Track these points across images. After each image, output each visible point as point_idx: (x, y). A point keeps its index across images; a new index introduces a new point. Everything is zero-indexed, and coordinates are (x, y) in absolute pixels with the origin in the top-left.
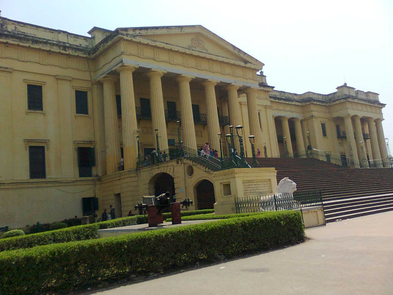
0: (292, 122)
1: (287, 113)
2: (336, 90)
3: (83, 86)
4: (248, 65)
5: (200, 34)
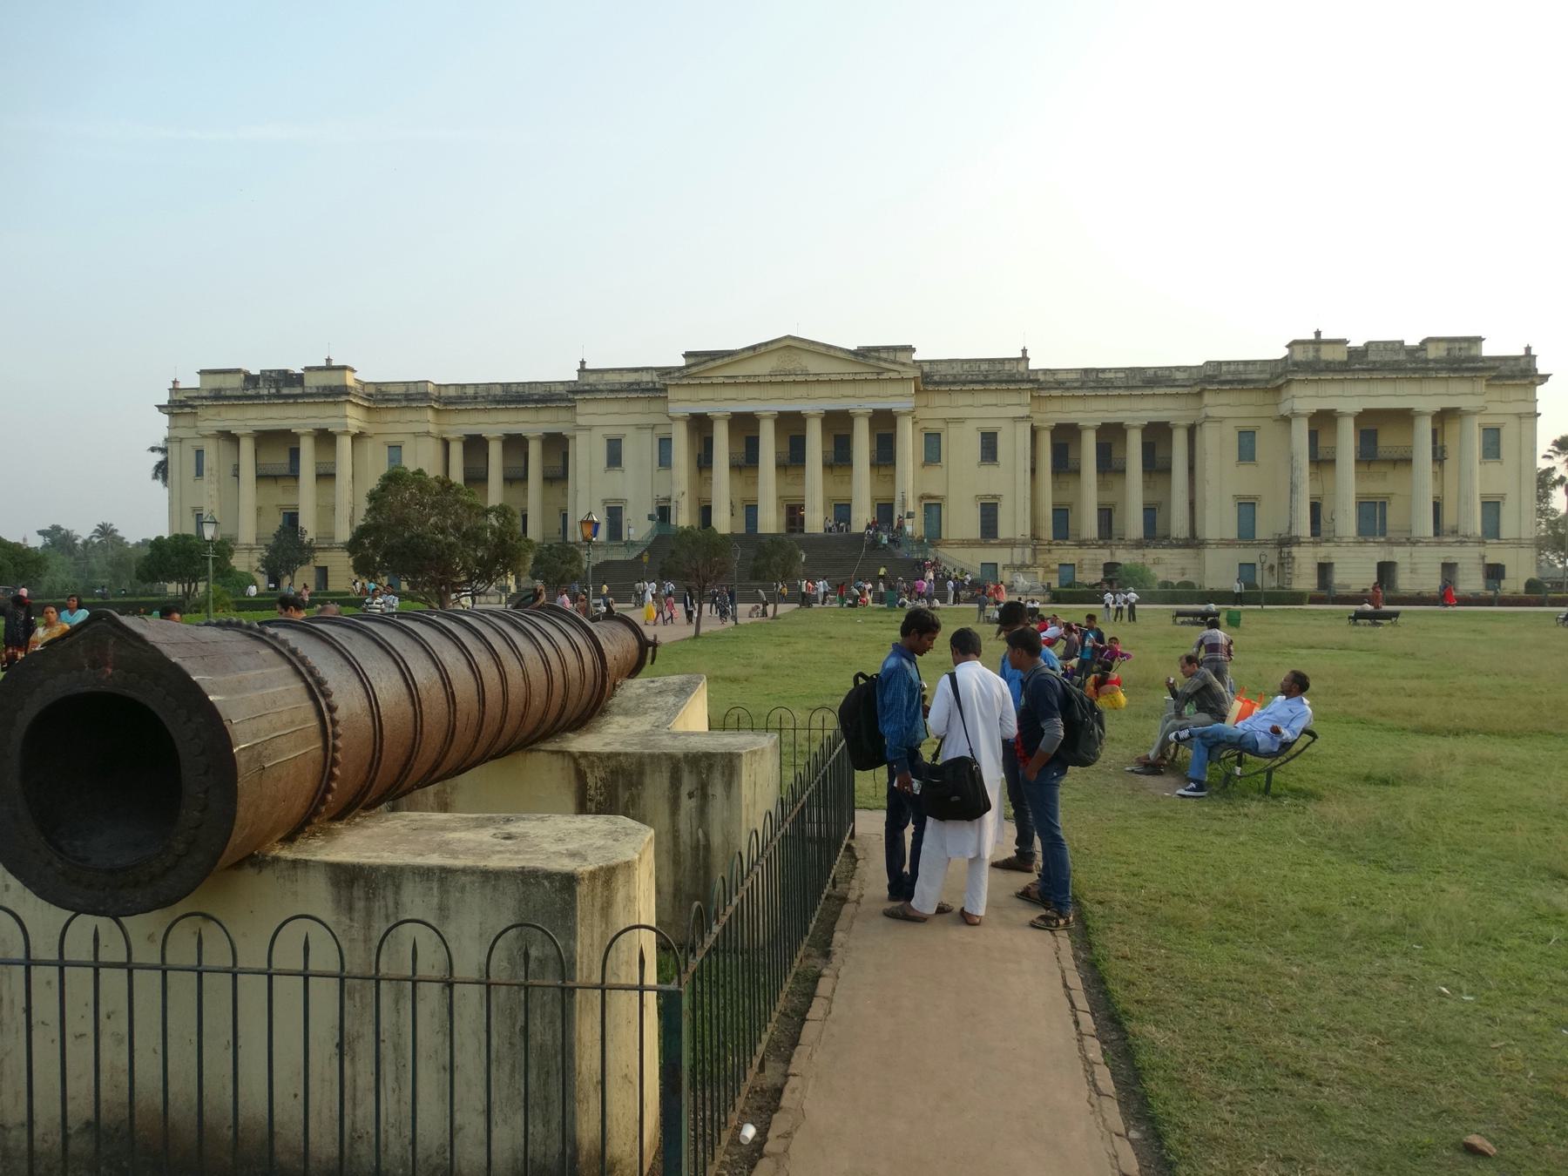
0: (1157, 434)
2: (1286, 352)
4: (885, 376)
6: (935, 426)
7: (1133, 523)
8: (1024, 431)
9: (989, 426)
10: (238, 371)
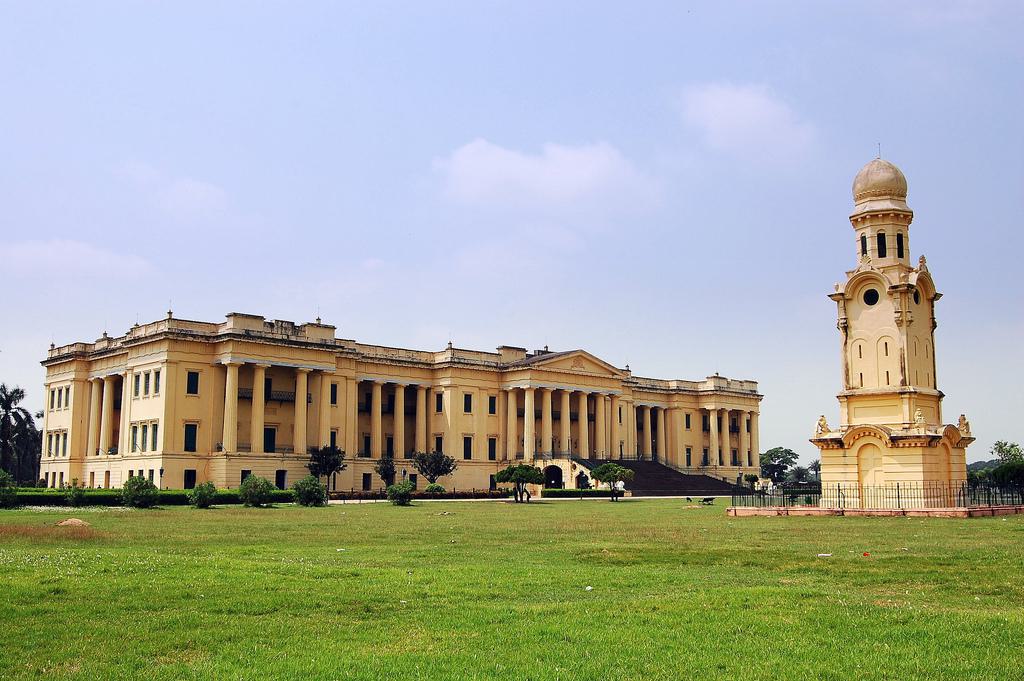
0: (654, 411)
1: (650, 402)
3: (493, 393)
5: (580, 357)
8: (631, 406)
10: (262, 318)
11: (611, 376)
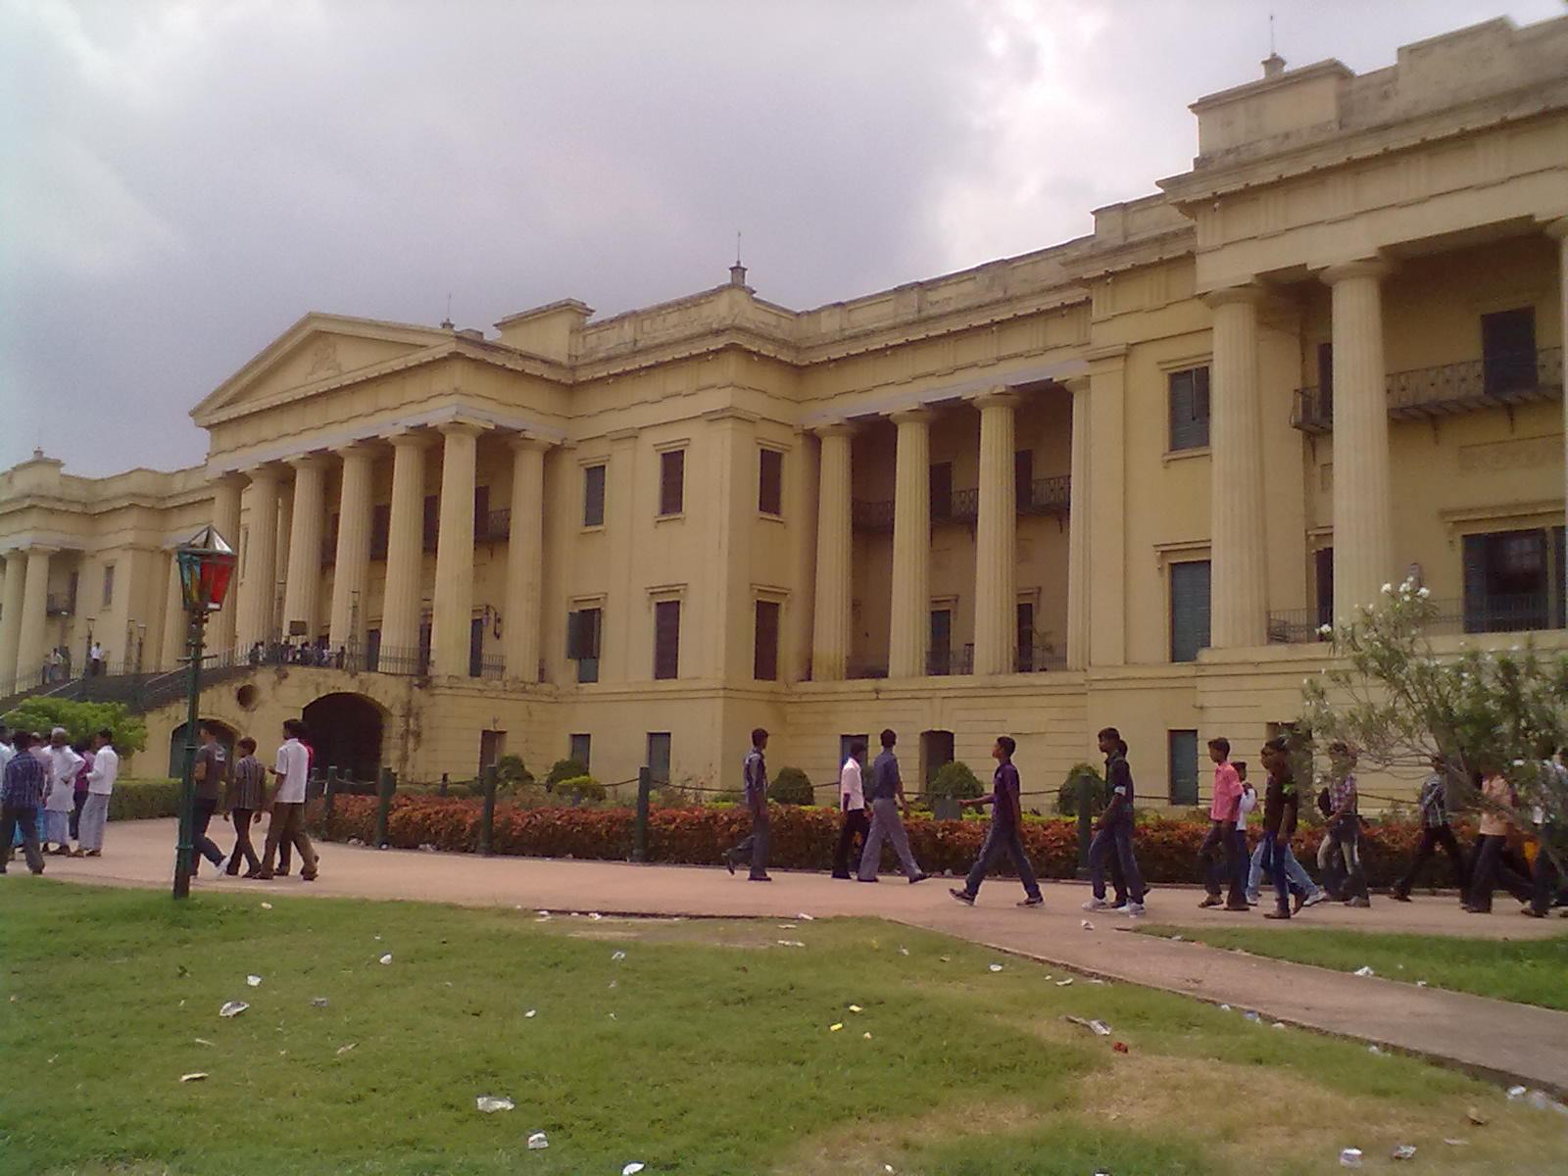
6: (595, 453)
7: (989, 626)
9: (670, 437)
11: (415, 358)
